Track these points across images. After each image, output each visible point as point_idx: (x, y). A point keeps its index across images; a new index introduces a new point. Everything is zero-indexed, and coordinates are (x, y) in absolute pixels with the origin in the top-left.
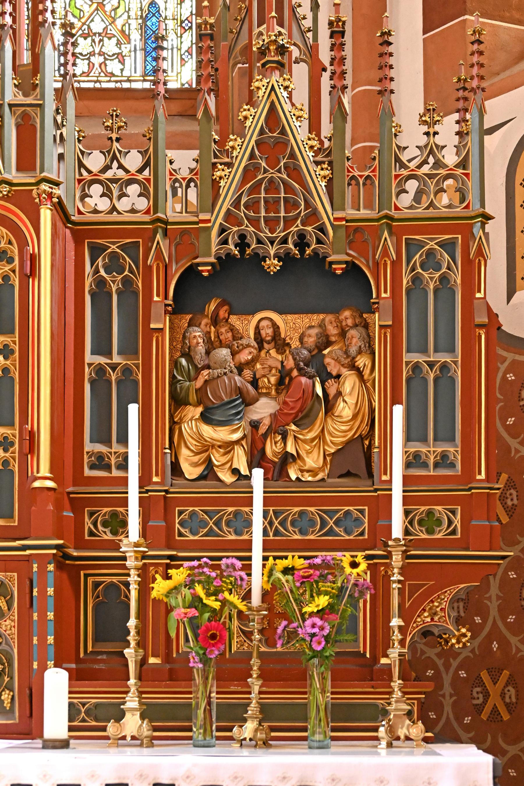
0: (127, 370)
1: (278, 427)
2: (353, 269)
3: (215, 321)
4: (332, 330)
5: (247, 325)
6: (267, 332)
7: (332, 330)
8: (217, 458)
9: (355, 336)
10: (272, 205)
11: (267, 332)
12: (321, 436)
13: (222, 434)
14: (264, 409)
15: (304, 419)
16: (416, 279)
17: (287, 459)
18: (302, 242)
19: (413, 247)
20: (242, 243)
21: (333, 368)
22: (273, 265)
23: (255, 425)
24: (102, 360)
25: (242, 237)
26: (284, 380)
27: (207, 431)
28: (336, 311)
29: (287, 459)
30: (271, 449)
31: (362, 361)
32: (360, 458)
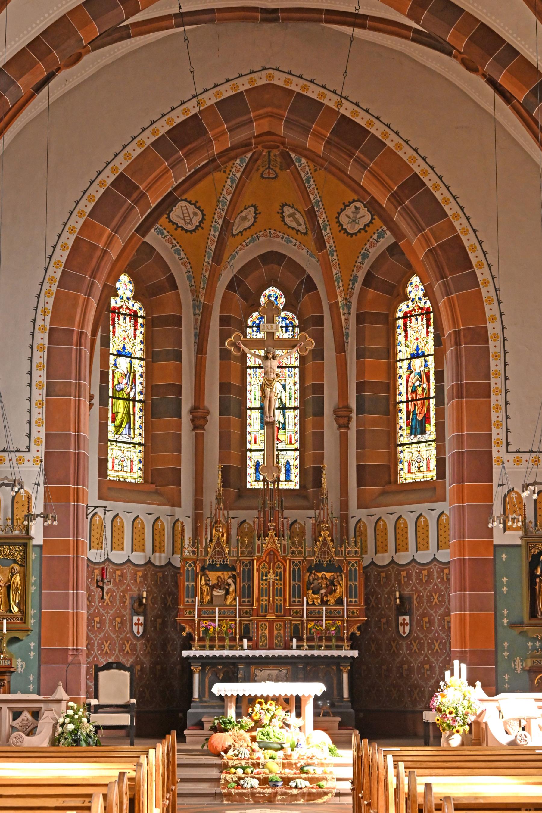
0: (299, 585)
3: (315, 574)
6: (324, 576)
8: (315, 600)
9: (340, 578)
10: (325, 555)
11: (324, 576)
13: (316, 596)
14: (323, 591)
15: (331, 593)
16: (351, 569)
17: (328, 601)
19: (350, 563)
20: (319, 561)
21: (336, 584)
22: (325, 565)
26: (327, 586)
28: (336, 572)
29: (328, 601)
30: (325, 599)
32: (340, 602)
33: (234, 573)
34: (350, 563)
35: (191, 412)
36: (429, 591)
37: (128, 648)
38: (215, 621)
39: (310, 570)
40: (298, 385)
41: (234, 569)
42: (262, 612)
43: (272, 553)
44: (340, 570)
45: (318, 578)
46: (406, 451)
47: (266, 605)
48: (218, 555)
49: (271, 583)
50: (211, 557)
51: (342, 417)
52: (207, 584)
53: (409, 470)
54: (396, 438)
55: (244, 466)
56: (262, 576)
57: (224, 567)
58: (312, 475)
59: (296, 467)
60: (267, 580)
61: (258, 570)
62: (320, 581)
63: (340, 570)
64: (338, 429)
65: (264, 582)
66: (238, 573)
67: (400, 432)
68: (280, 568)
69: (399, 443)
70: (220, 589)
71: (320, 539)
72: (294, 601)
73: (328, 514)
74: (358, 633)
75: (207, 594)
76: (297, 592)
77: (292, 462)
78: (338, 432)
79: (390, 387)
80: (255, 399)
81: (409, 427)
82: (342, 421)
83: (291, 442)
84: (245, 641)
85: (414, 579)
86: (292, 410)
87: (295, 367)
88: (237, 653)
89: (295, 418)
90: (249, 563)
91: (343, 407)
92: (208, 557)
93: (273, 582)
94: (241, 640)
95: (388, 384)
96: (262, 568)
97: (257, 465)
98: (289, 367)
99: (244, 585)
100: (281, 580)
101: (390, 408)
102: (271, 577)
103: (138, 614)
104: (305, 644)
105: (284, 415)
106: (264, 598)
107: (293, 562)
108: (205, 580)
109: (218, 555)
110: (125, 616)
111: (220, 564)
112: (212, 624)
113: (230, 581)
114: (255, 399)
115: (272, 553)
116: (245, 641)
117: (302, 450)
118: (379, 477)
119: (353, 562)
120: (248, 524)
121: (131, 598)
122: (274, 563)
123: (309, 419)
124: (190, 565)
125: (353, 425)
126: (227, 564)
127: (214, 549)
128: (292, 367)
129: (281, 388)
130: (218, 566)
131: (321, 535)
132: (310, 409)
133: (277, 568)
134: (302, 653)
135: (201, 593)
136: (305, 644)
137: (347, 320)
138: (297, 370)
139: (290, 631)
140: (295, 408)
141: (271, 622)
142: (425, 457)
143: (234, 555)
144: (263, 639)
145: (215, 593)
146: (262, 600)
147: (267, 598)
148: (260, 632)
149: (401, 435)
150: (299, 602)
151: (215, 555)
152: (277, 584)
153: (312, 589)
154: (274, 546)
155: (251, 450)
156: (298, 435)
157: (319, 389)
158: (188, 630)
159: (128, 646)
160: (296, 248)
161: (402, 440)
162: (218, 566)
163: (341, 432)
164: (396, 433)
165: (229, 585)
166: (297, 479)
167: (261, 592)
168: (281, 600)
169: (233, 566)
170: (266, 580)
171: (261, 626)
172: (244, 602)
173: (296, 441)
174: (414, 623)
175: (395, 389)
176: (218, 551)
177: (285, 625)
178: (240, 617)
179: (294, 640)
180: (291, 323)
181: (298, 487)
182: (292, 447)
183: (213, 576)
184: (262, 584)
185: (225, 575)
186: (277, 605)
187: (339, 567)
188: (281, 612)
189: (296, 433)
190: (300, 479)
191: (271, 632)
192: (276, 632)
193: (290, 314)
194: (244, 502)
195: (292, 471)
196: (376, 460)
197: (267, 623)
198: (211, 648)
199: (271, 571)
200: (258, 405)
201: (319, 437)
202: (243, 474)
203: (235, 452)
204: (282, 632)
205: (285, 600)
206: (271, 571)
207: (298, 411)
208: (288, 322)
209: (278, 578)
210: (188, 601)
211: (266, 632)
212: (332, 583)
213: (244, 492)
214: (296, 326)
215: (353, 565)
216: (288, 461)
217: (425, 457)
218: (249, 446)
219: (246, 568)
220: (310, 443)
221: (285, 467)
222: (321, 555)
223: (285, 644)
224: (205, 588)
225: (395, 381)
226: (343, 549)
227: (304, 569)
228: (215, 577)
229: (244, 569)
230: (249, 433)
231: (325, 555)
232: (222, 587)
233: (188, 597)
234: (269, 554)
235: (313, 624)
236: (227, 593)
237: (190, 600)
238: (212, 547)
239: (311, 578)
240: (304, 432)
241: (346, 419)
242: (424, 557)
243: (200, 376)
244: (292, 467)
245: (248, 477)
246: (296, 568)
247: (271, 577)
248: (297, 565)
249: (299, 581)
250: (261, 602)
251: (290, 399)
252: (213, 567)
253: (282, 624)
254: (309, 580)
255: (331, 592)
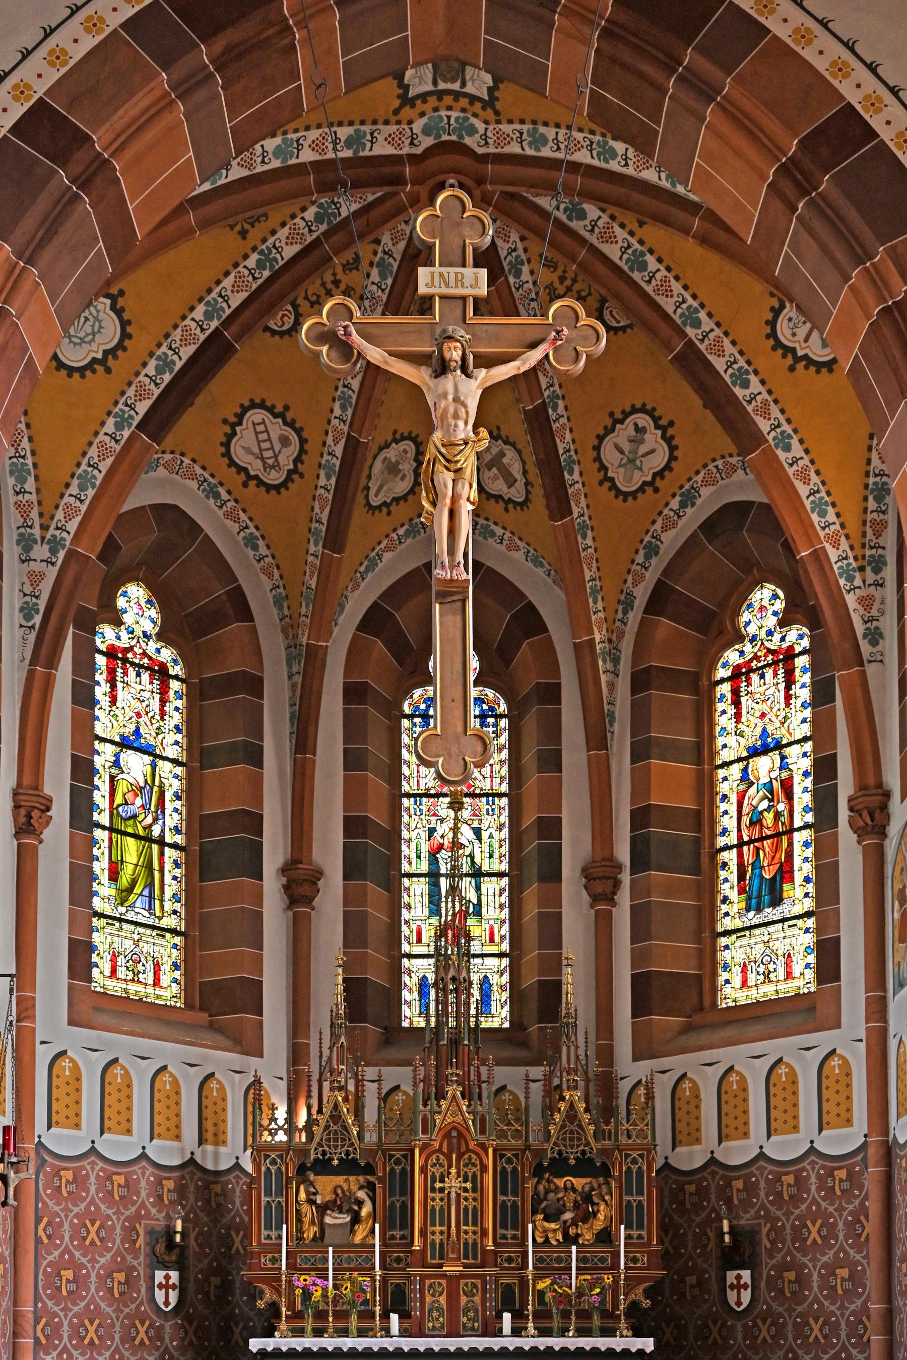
1: (574, 1223)
2: (604, 1164)
3: (548, 1181)
4: (596, 1186)
5: (560, 1182)
7: (596, 1186)
8: (550, 1235)
10: (572, 1139)
12: (591, 1227)
13: (553, 1226)
14: (568, 1216)
15: (585, 1220)
16: (629, 1169)
17: (578, 1236)
18: (583, 1153)
19: (627, 1156)
21: (596, 1200)
23: (565, 1222)
24: (505, 1198)
25: (560, 1151)
26: (576, 1206)
27: (546, 1224)
29: (578, 1236)
30: (572, 1231)
31: (607, 1198)
32: (606, 1237)
33: (371, 1178)
34: (627, 1156)
35: (284, 870)
36: (798, 1218)
37: (142, 1335)
38: (326, 1279)
39: (538, 1172)
40: (506, 831)
41: (369, 1169)
42: (433, 1257)
43: (455, 1137)
44: (605, 1171)
45: (557, 1189)
46: (738, 944)
47: (441, 1244)
48: (336, 1140)
49: (453, 1195)
50: (320, 1144)
51: (601, 881)
52: (311, 1202)
53: (744, 983)
54: (713, 921)
55: (398, 986)
56: (434, 1181)
57: (349, 1166)
58: (538, 999)
59: (502, 988)
60: (444, 1191)
61: (423, 1170)
62: (561, 1195)
63: (605, 1171)
64: (592, 907)
65: (438, 1195)
66: (378, 1178)
67: (724, 908)
68: (474, 1165)
69: (720, 929)
70: (341, 1212)
71: (563, 1106)
72: (504, 1237)
73: (577, 1057)
74: (646, 1303)
75: (312, 1222)
76: (511, 1218)
77: (494, 979)
78: (593, 912)
79: (703, 818)
80: (419, 857)
81: (744, 896)
82: (599, 887)
83: (492, 940)
84: (394, 1317)
85: (762, 1194)
86: (494, 879)
87: (500, 795)
88: (375, 1343)
89: (501, 894)
90: (405, 1156)
91: (603, 860)
92: (313, 1145)
93: (458, 1195)
94: (385, 1317)
95: (698, 814)
96: (434, 1165)
97: (423, 984)
98: (487, 795)
99: (392, 1203)
100: (474, 1190)
101: (701, 862)
102: (453, 1184)
103: (165, 1266)
104: (531, 1324)
105: (478, 889)
106: (438, 1228)
107: (502, 1156)
108: (308, 1193)
109: (336, 1140)
110: (134, 1268)
111: (341, 1160)
112: (318, 1281)
113: (361, 1194)
114: (419, 857)
115: (454, 1134)
116: (394, 1317)
117: (515, 956)
118: (680, 1000)
119: (634, 1154)
120: (405, 1093)
121: (150, 1232)
122: (460, 1156)
123: (531, 892)
124: (274, 1162)
125: (624, 898)
126: (354, 1160)
127: (327, 1127)
128: (494, 795)
129: (471, 835)
130: (336, 1162)
131: (562, 1098)
132: (532, 871)
133: (466, 1165)
134: (525, 1343)
135: (299, 1220)
136: (531, 1324)
137: (612, 686)
138: (504, 801)
139: (494, 1298)
140: (500, 875)
141: (453, 1280)
142: (780, 952)
143: (371, 1138)
144: (435, 1314)
145: (328, 1220)
146: (433, 1233)
147: (445, 1228)
148: (428, 1299)
149: (727, 914)
150: (514, 1237)
151: (329, 1140)
152: (466, 1199)
153: (544, 1211)
154: (459, 1119)
155: (410, 956)
156: (506, 927)
157: (551, 828)
158: (269, 1295)
159: (142, 1330)
160: (502, 548)
161: (728, 924)
162: (336, 1162)
163: (597, 911)
164: (713, 909)
165: (360, 1203)
166: (505, 1012)
167: (429, 1215)
168: (475, 1233)
169: (368, 1164)
170: (442, 1190)
171: (431, 1286)
172: (393, 1237)
173: (503, 938)
174: (763, 1284)
175: (713, 822)
176: (336, 1133)
177: (484, 1284)
178: (383, 1266)
179: (507, 1316)
180: (492, 709)
181: (507, 1025)
182: (494, 949)
183: (326, 1186)
184: (433, 1199)
185: (353, 1184)
186: (466, 1244)
187: (604, 1164)
188: (475, 1258)
189: (503, 922)
190: (511, 1011)
191: (453, 1299)
192: (464, 1299)
193: (490, 693)
194: (392, 1053)
195: (495, 996)
196: (673, 957)
197: (444, 1282)
198: (319, 1333)
199: (453, 1170)
200: (424, 866)
201: (551, 926)
202: (394, 1002)
203: (376, 955)
204: (477, 1299)
205: (484, 1233)
206: (453, 1170)
207: (505, 881)
208: (485, 707)
209: (469, 1185)
210: (269, 1237)
211: (443, 1300)
212: (587, 1198)
213: (393, 1034)
214: (501, 716)
215: (634, 1161)
216: (486, 977)
217: (780, 952)
218: (405, 948)
219: (398, 1169)
220: (534, 938)
221: (481, 989)
222: (564, 1139)
223: (485, 1324)
224: (306, 1208)
225: (713, 806)
226: (611, 1127)
227: (527, 1168)
228: (330, 1188)
229: (392, 1169)
230: (406, 922)
231: (572, 1139)
232: (345, 1208)
233: (268, 1227)
234: (448, 1135)
235: (548, 1281)
236: (356, 1219)
237: (273, 1234)
238: (323, 1123)
239: (541, 1188)
240: (520, 919)
241: (610, 882)
242: (785, 1148)
243: (303, 789)
244: (495, 988)
245: (405, 1008)
246: (509, 1168)
247: (453, 1184)
248: (509, 1161)
249: (515, 1193)
250: (430, 1237)
251: (491, 856)
252: (323, 1166)
253: (479, 1282)
254: (536, 1193)
255: (587, 1217)
